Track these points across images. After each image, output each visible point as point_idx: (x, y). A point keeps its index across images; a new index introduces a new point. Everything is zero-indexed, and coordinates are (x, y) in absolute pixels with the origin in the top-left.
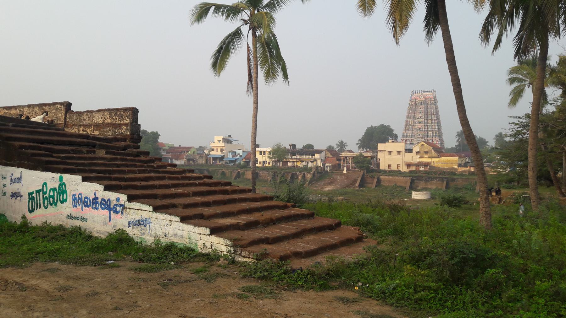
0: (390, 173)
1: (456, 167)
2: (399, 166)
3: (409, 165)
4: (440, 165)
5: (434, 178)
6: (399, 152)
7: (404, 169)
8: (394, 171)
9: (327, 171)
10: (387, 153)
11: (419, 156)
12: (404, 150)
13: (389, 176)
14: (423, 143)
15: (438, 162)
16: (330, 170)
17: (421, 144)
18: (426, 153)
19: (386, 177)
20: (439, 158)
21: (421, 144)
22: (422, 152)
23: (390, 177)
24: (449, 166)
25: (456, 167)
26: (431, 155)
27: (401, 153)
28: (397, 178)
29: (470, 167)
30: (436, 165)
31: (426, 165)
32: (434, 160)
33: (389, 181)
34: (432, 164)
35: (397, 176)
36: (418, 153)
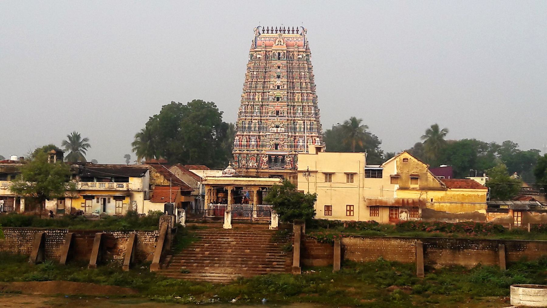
0: (354, 227)
1: (483, 211)
2: (350, 209)
3: (374, 207)
4: (446, 207)
5: (473, 242)
6: (350, 176)
7: (362, 215)
8: (360, 223)
9: (180, 226)
10: (323, 177)
11: (397, 186)
12: (362, 172)
13: (364, 237)
14: (407, 155)
15: (441, 200)
16: (186, 222)
17: (402, 157)
18: (414, 178)
19: (358, 241)
20: (443, 189)
21: (402, 157)
22: (404, 176)
23: (368, 241)
24: (467, 209)
25: (483, 211)
26: (424, 184)
27: (355, 178)
28: (384, 242)
29: (514, 211)
30: (436, 206)
31: (413, 207)
32: (431, 195)
33: (366, 251)
34: (429, 205)
35: (384, 238)
36: (394, 178)
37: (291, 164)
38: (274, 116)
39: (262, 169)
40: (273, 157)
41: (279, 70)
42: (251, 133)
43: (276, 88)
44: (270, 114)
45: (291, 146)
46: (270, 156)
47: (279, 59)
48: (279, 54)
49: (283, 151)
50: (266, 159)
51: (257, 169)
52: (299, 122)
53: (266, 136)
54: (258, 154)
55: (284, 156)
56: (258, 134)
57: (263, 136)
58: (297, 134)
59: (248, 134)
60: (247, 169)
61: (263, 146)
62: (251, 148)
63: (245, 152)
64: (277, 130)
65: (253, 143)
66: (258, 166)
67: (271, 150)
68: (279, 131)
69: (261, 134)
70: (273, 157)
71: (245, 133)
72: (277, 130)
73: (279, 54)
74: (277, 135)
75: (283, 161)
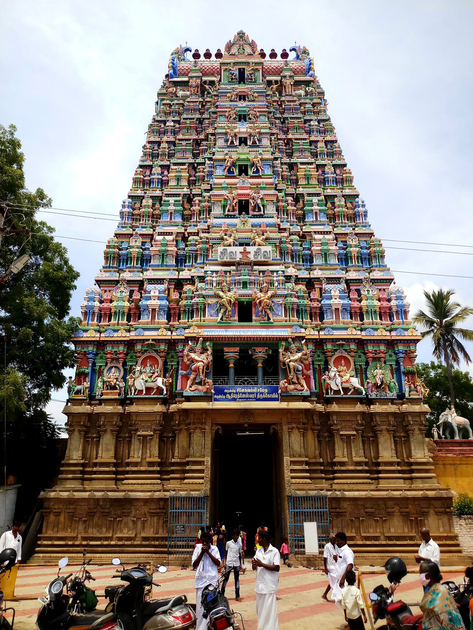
37: (307, 379)
38: (234, 217)
39: (189, 399)
40: (231, 354)
41: (242, 104)
42: (150, 274)
43: (237, 143)
44: (217, 211)
45: (299, 311)
46: (219, 346)
47: (242, 79)
48: (242, 72)
49: (268, 325)
50: (202, 359)
51: (165, 402)
52: (317, 237)
53: (202, 279)
54: (172, 343)
55: (273, 344)
56: (174, 275)
57: (191, 281)
58: (317, 273)
59: (138, 276)
60: (124, 401)
61: (191, 312)
62: (145, 319)
63: (122, 335)
64: (245, 253)
65: (154, 303)
66: (170, 386)
67: (224, 324)
68: (252, 257)
69: (185, 274)
70: (231, 354)
71: (127, 275)
72: (245, 253)
73: (242, 72)
74: (245, 270)
75: (273, 368)
